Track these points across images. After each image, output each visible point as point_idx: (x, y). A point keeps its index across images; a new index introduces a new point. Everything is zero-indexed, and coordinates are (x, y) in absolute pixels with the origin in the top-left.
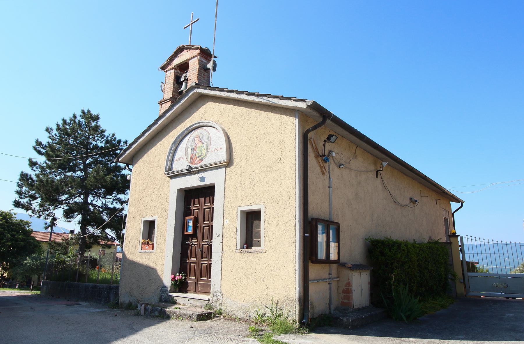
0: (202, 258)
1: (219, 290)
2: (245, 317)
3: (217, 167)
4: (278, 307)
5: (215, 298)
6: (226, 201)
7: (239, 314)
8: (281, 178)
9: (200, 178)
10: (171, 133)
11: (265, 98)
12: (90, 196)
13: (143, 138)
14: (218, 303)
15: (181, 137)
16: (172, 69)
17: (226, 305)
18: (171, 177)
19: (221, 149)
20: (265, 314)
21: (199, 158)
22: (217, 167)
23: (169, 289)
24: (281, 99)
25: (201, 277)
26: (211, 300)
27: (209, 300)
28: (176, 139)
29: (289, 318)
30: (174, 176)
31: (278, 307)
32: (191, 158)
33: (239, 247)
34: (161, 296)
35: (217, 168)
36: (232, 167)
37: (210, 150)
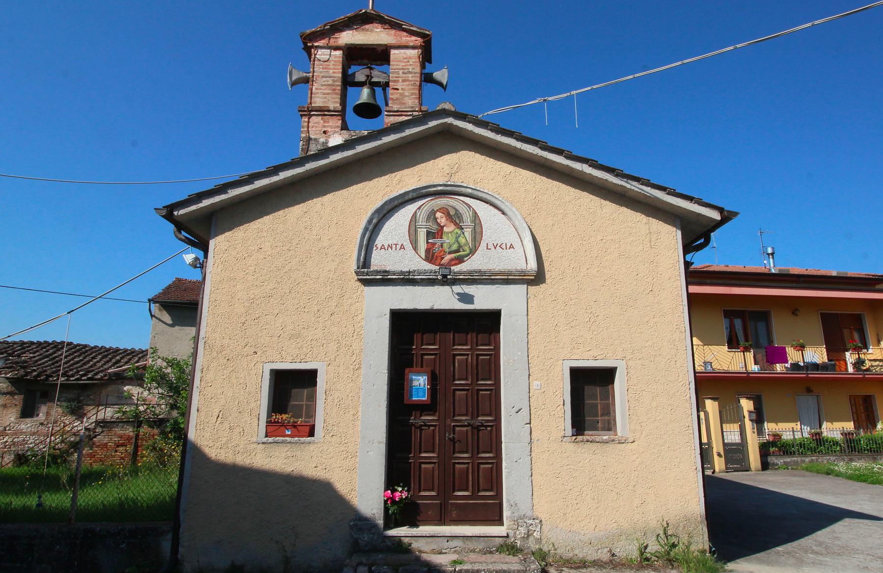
0: (454, 453)
1: (529, 513)
2: (605, 556)
3: (507, 279)
4: (670, 533)
5: (523, 530)
6: (532, 347)
7: (591, 555)
8: (655, 320)
9: (458, 294)
10: (355, 187)
12: (848, 354)
13: (275, 179)
14: (531, 539)
15: (396, 203)
16: (336, 48)
17: (553, 540)
18: (367, 283)
19: (512, 247)
20: (646, 547)
21: (453, 255)
22: (507, 279)
23: (381, 522)
24: (668, 194)
25: (479, 491)
26: (511, 535)
27: (508, 536)
28: (386, 203)
29: (693, 548)
30: (385, 279)
31: (670, 533)
32: (428, 251)
33: (569, 430)
34: (356, 540)
35: (507, 282)
36: (543, 286)
37: (483, 245)
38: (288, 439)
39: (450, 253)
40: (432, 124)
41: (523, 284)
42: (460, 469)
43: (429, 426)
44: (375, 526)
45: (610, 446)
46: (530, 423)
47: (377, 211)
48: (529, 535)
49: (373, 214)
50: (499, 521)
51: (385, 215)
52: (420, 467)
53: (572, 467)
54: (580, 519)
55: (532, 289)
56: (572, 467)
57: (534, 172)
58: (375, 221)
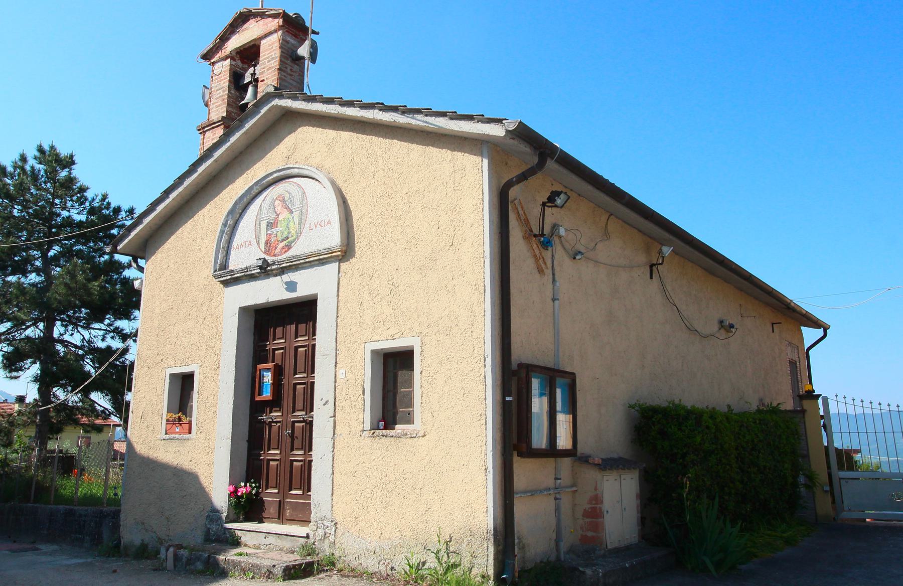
0: (292, 450)
1: (329, 515)
2: (384, 570)
4: (451, 549)
5: (320, 532)
6: (340, 331)
7: (371, 564)
8: (455, 282)
9: (286, 283)
10: (224, 192)
11: (420, 117)
12: (58, 323)
13: (167, 201)
14: (326, 541)
16: (226, 58)
17: (344, 546)
18: (226, 283)
19: (329, 223)
20: (424, 563)
21: (284, 243)
23: (224, 515)
24: (451, 119)
25: (290, 489)
26: (311, 536)
27: (308, 537)
28: (236, 203)
29: (475, 571)
30: (232, 281)
31: (451, 549)
32: (267, 242)
33: (368, 426)
34: (209, 529)
35: (322, 262)
36: (353, 260)
37: (307, 226)
38: (177, 436)
39: (282, 241)
40: (264, 110)
41: (335, 262)
42: (297, 467)
43: (277, 422)
44: (220, 518)
45: (403, 440)
46: (334, 416)
47: (231, 212)
48: (325, 536)
49: (227, 216)
50: (306, 522)
51: (241, 214)
52: (268, 464)
53: (367, 465)
54: (369, 524)
55: (344, 266)
56: (367, 465)
57: (352, 131)
58: (230, 222)
